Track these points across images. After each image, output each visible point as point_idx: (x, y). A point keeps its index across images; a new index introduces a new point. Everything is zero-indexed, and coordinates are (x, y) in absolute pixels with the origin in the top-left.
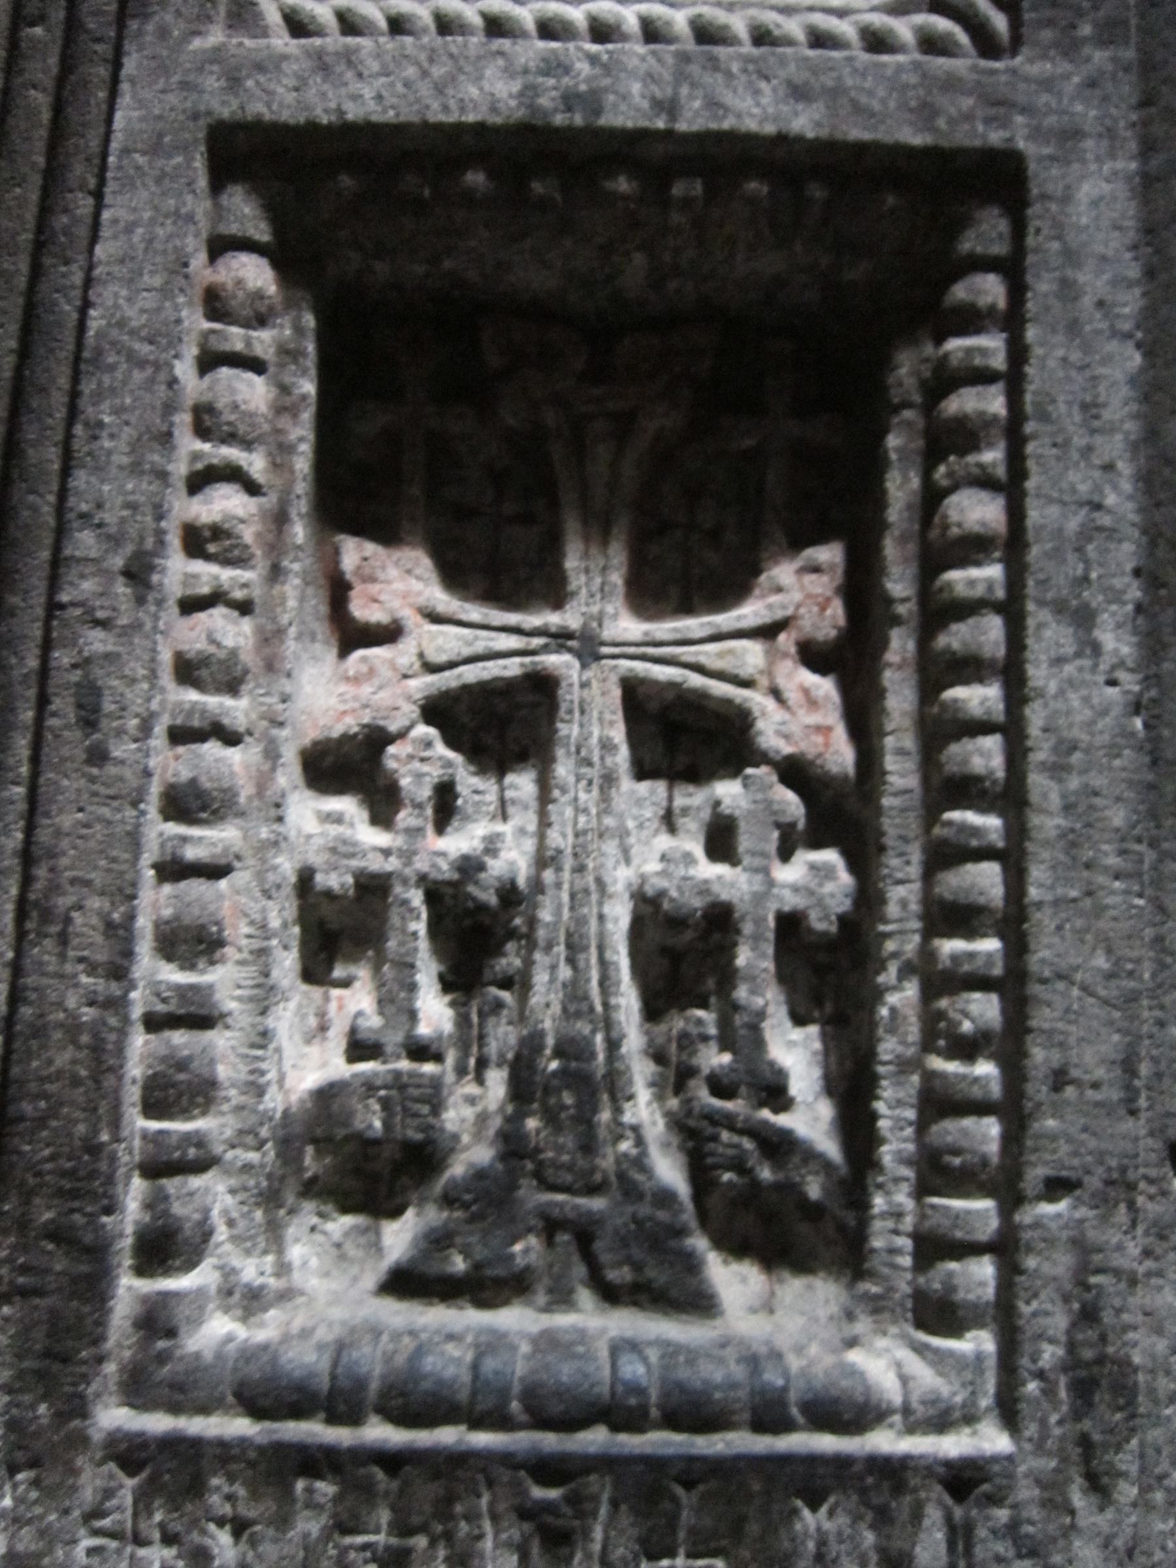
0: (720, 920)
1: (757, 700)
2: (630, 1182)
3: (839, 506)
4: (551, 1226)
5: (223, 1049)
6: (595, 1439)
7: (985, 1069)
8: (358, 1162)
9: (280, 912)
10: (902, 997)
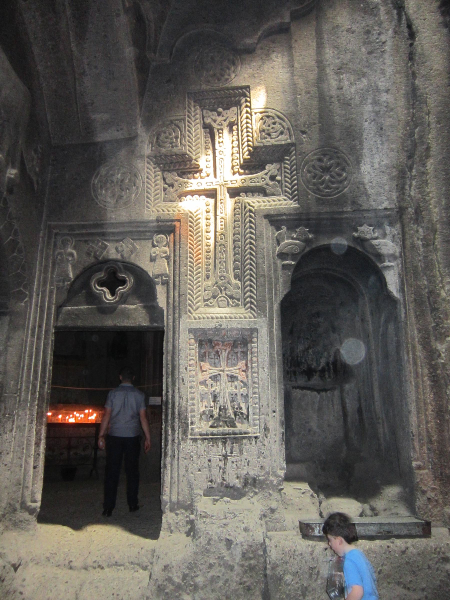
1: (238, 375)
2: (229, 417)
4: (223, 421)
5: (195, 407)
9: (199, 396)
10: (251, 400)
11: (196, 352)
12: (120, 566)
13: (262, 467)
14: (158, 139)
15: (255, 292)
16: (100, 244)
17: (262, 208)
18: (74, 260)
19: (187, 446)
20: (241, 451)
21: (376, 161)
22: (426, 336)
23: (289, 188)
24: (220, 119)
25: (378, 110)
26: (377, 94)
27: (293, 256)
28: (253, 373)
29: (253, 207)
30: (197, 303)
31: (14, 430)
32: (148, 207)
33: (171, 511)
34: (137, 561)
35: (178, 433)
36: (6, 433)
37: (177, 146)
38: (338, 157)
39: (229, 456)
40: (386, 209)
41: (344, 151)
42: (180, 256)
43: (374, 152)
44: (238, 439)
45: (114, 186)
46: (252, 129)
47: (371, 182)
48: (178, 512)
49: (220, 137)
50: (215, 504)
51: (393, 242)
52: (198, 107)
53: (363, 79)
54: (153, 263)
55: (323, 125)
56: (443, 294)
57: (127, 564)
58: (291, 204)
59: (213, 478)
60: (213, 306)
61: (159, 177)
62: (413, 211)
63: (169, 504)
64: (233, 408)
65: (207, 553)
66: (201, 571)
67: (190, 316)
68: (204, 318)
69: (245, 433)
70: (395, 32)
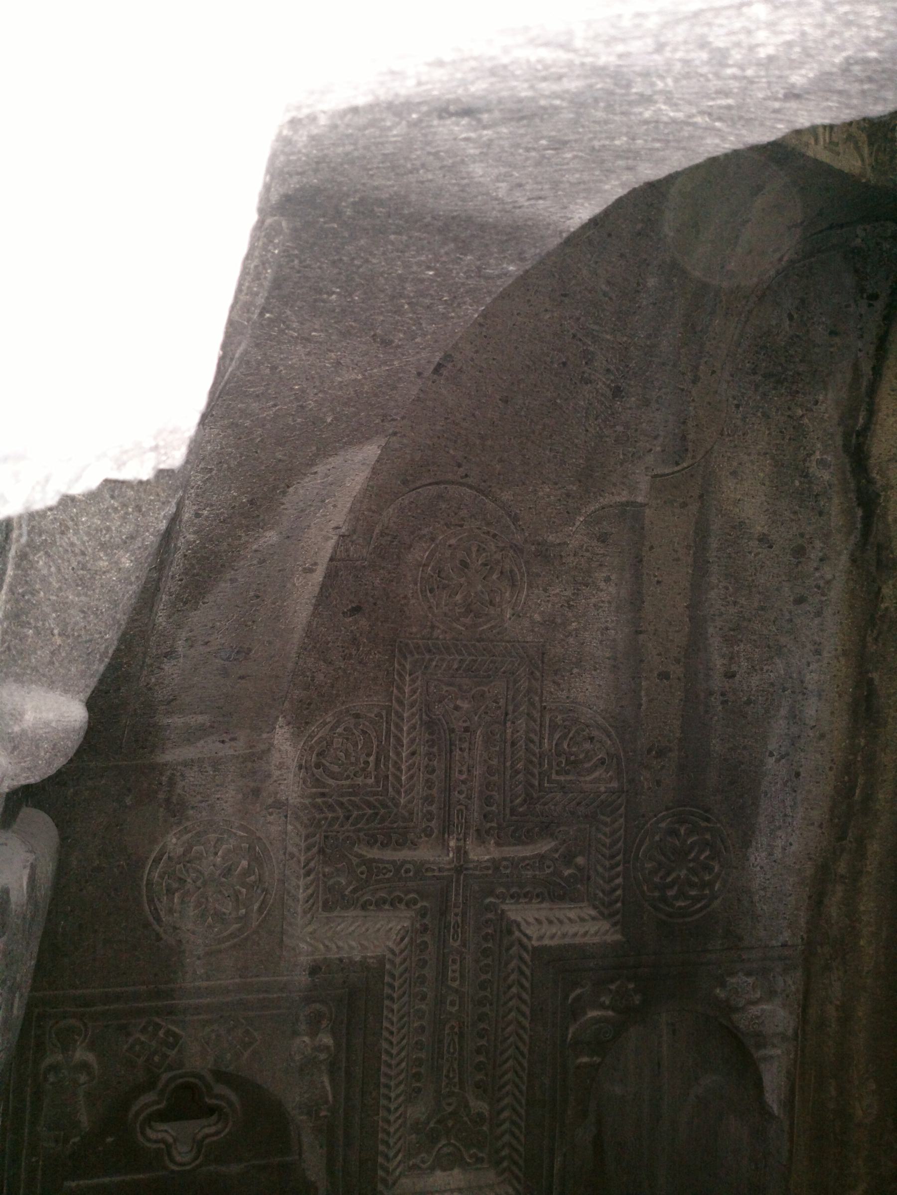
15: (522, 1138)
16: (161, 1034)
17: (546, 942)
21: (779, 843)
23: (603, 891)
26: (800, 697)
29: (529, 938)
40: (784, 945)
45: (205, 884)
47: (764, 889)
55: (687, 757)
58: (607, 931)
70: (853, 561)
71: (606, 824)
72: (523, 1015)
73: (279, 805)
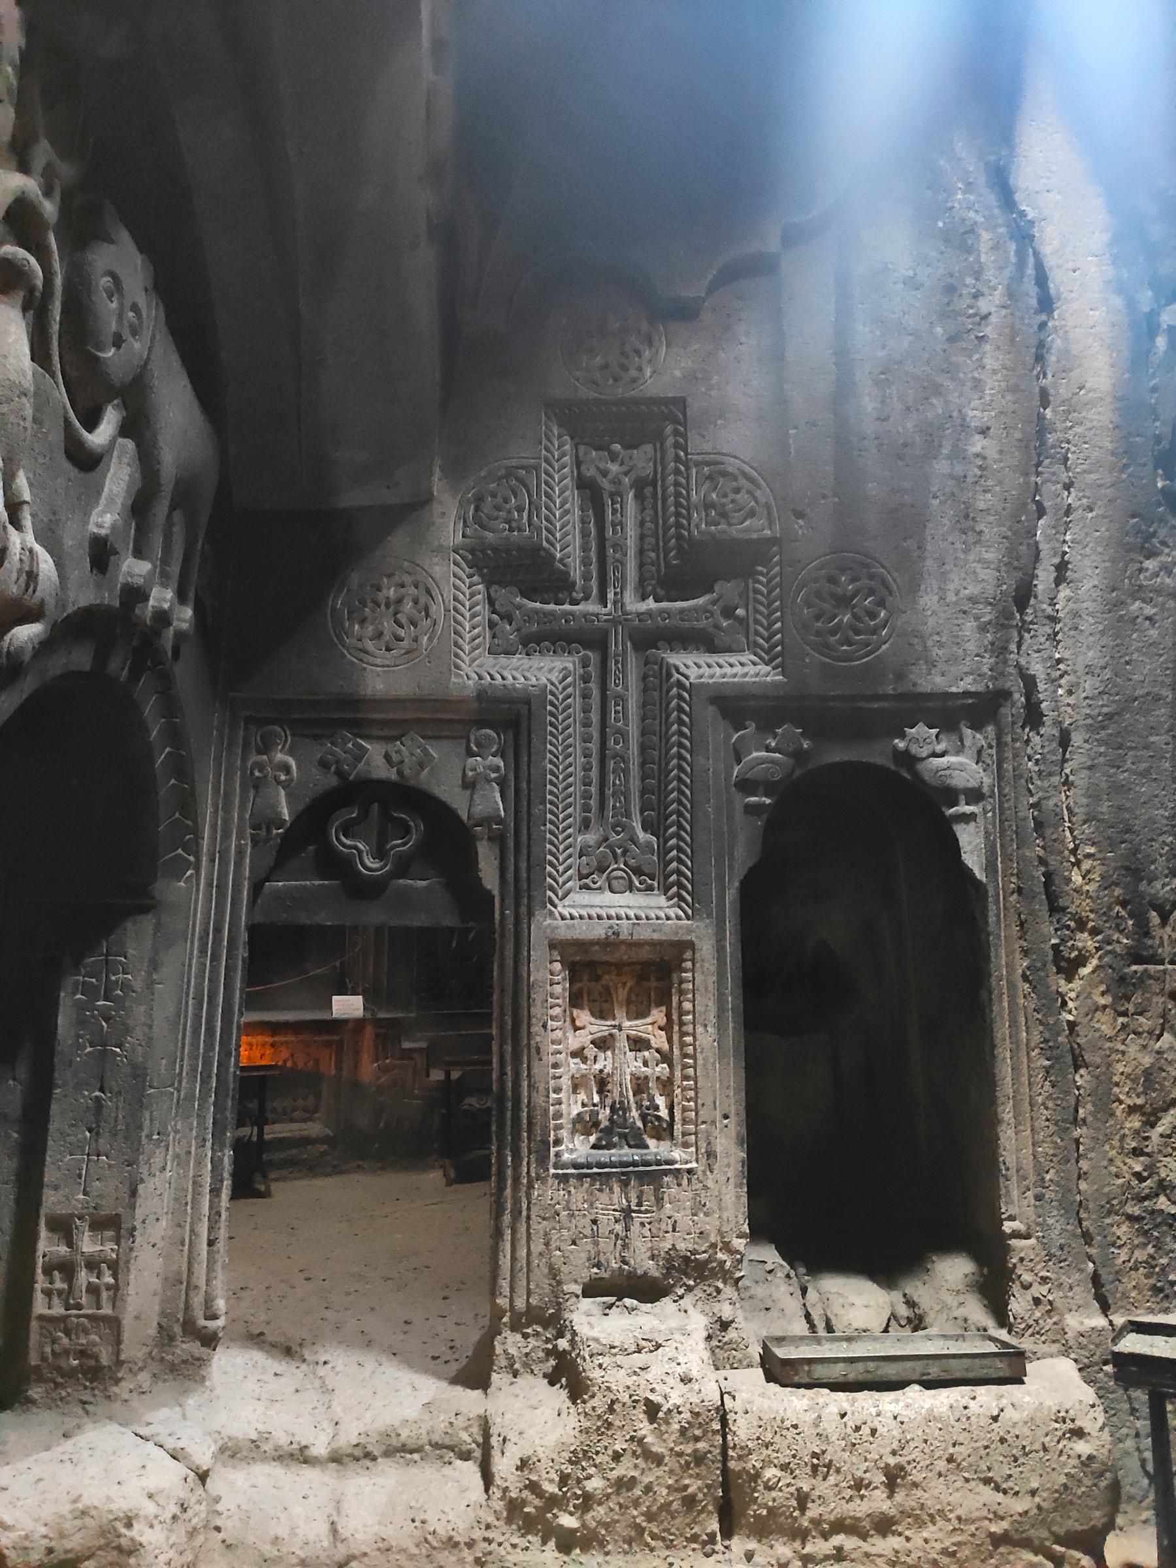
0: (646, 1078)
2: (633, 1126)
3: (664, 999)
4: (621, 1136)
5: (563, 1106)
6: (631, 1169)
7: (692, 1103)
8: (585, 1124)
10: (678, 1091)
11: (564, 989)
12: (411, 1452)
13: (701, 1233)
14: (477, 509)
16: (350, 745)
18: (292, 780)
19: (548, 1193)
20: (659, 1200)
21: (951, 586)
22: (1039, 965)
24: (614, 468)
25: (962, 474)
27: (768, 788)
28: (683, 1034)
29: (687, 678)
30: (565, 883)
31: (168, 1168)
32: (457, 667)
33: (513, 1329)
34: (447, 1441)
35: (528, 1163)
36: (154, 1175)
37: (520, 530)
38: (871, 577)
39: (634, 1211)
40: (966, 694)
41: (885, 562)
42: (529, 782)
43: (947, 567)
44: (652, 1176)
46: (688, 498)
47: (938, 633)
48: (529, 1331)
49: (614, 511)
50: (606, 1315)
51: (977, 763)
52: (567, 438)
53: (934, 401)
54: (468, 792)
56: (1077, 878)
57: (427, 1447)
59: (603, 1260)
60: (600, 888)
61: (480, 597)
62: (1023, 699)
63: (508, 1314)
64: (639, 1106)
65: (608, 1429)
66: (595, 1466)
67: (551, 913)
68: (581, 917)
69: (668, 1162)
71: (762, 574)
72: (684, 747)
73: (440, 550)
